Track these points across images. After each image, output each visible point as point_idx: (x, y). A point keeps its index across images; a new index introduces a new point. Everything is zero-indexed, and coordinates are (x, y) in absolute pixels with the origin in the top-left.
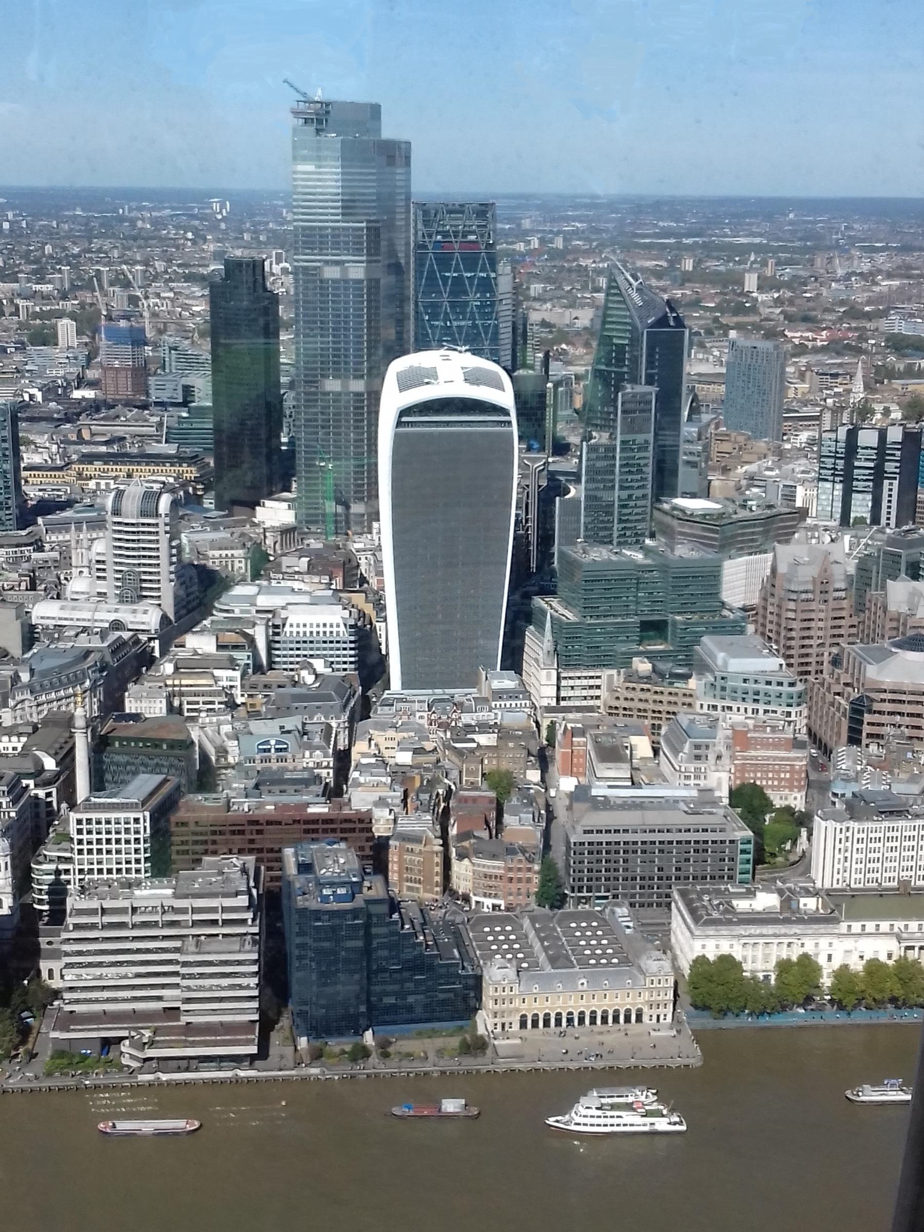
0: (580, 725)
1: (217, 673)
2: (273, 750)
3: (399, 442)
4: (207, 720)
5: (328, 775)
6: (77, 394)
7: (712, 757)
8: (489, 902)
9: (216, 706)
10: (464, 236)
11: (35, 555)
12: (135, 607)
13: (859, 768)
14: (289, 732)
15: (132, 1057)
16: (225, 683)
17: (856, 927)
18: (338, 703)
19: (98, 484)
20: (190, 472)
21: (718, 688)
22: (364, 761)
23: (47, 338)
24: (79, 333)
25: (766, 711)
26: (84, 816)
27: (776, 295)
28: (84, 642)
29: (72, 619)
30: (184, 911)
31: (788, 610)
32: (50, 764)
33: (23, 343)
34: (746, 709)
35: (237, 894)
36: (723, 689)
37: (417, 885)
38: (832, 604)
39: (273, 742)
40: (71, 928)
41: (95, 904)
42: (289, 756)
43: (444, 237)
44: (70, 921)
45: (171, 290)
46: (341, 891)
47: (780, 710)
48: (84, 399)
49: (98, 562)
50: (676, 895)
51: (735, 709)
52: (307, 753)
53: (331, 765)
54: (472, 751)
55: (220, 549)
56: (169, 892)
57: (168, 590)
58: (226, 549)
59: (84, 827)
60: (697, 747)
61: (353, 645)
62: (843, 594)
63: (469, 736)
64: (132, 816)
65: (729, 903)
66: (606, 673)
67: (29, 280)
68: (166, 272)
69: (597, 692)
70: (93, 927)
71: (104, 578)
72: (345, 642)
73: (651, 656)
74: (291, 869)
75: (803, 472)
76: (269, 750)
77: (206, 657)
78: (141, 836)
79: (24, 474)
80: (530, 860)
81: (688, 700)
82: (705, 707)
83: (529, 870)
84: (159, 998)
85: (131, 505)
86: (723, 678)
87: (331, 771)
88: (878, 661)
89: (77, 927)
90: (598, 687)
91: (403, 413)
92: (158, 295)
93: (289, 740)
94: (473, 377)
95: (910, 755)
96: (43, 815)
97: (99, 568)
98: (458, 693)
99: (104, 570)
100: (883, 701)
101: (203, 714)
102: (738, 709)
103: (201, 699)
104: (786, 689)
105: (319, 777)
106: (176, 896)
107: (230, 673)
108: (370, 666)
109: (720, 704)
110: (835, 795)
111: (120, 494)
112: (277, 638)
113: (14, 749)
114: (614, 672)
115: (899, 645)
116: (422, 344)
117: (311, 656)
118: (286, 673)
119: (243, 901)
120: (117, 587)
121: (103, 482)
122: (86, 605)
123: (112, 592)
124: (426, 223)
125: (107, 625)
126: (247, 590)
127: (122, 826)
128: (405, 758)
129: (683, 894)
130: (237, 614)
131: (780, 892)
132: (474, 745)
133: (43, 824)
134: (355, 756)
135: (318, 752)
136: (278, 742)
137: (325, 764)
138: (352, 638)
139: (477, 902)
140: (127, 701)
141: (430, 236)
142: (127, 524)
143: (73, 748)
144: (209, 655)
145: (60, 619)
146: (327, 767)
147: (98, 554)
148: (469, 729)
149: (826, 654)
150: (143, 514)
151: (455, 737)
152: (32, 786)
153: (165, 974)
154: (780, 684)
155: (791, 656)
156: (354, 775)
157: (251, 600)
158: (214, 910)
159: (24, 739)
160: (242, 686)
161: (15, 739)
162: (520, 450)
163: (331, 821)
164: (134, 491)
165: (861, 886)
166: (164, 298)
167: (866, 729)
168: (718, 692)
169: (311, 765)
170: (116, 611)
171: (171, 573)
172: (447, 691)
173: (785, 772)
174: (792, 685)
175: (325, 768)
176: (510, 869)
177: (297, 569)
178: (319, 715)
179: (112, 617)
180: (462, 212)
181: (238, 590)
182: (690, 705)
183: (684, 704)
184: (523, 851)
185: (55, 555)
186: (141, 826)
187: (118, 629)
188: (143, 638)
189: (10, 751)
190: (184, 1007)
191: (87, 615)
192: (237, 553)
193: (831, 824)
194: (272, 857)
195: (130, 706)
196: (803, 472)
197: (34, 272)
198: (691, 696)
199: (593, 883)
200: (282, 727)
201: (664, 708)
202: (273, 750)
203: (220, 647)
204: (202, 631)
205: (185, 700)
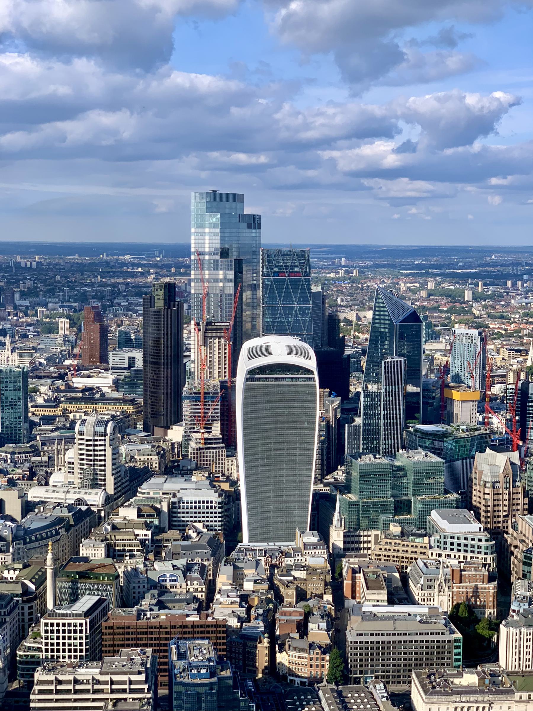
0: (357, 566)
2: (168, 581)
3: (247, 390)
5: (202, 596)
6: (67, 362)
7: (437, 587)
10: (292, 269)
11: (34, 459)
12: (91, 490)
14: (178, 569)
16: (141, 537)
17: (525, 696)
19: (75, 416)
20: (130, 409)
21: (442, 543)
22: (224, 588)
23: (52, 329)
24: (71, 326)
25: (471, 558)
26: (49, 621)
28: (58, 513)
29: (52, 498)
30: (106, 683)
31: (484, 494)
32: (33, 587)
33: (38, 332)
34: (459, 556)
35: (139, 673)
36: (445, 543)
39: (168, 576)
40: (37, 692)
41: (51, 677)
42: (178, 584)
43: (279, 269)
44: (36, 688)
45: (127, 301)
46: (203, 671)
47: (480, 556)
49: (69, 463)
50: (414, 675)
51: (453, 556)
52: (189, 582)
53: (204, 590)
55: (144, 455)
56: (98, 670)
58: (148, 455)
59: (49, 628)
60: (429, 580)
61: (220, 515)
64: (78, 622)
66: (374, 533)
67: (44, 296)
68: (125, 291)
69: (370, 545)
70: (50, 692)
71: (73, 473)
72: (215, 513)
73: (401, 523)
76: (166, 581)
77: (130, 521)
78: (83, 635)
79: (33, 410)
80: (324, 653)
81: (423, 550)
82: (434, 555)
87: (203, 594)
89: (41, 692)
90: (369, 542)
91: (252, 372)
92: (119, 304)
93: (179, 573)
94: (291, 350)
96: (26, 620)
98: (284, 545)
99: (73, 468)
102: (455, 556)
105: (195, 597)
106: (101, 673)
107: (145, 532)
108: (232, 529)
109: (444, 553)
110: (514, 611)
112: (174, 510)
113: (11, 578)
114: (379, 532)
116: (268, 331)
117: (195, 521)
119: (142, 677)
121: (78, 415)
122: (62, 489)
123: (77, 481)
124: (269, 262)
125: (73, 502)
127: (72, 628)
129: (418, 675)
130: (151, 495)
131: (478, 674)
132: (292, 578)
133: (26, 626)
134: (219, 586)
135: (195, 582)
136: (171, 575)
137: (200, 589)
139: (291, 680)
140: (81, 549)
141: (271, 269)
142: (87, 440)
143: (45, 579)
144: (133, 520)
145: (45, 498)
146: (202, 591)
147: (69, 458)
151: (280, 573)
152: (20, 602)
156: (217, 596)
158: (123, 683)
161: (12, 572)
162: (322, 395)
166: (122, 306)
170: (79, 493)
172: (277, 544)
174: (486, 541)
175: (200, 592)
176: (312, 659)
177: (189, 467)
179: (77, 496)
180: (290, 255)
181: (153, 480)
183: (421, 553)
184: (320, 647)
185: (45, 458)
186: (84, 628)
187: (79, 504)
188: (95, 510)
191: (62, 496)
192: (154, 458)
193: (513, 630)
194: (161, 649)
195: (83, 552)
197: (48, 291)
198: (425, 547)
199: (363, 668)
200: (174, 566)
201: (409, 555)
202: (168, 581)
203: (139, 516)
204: (130, 505)
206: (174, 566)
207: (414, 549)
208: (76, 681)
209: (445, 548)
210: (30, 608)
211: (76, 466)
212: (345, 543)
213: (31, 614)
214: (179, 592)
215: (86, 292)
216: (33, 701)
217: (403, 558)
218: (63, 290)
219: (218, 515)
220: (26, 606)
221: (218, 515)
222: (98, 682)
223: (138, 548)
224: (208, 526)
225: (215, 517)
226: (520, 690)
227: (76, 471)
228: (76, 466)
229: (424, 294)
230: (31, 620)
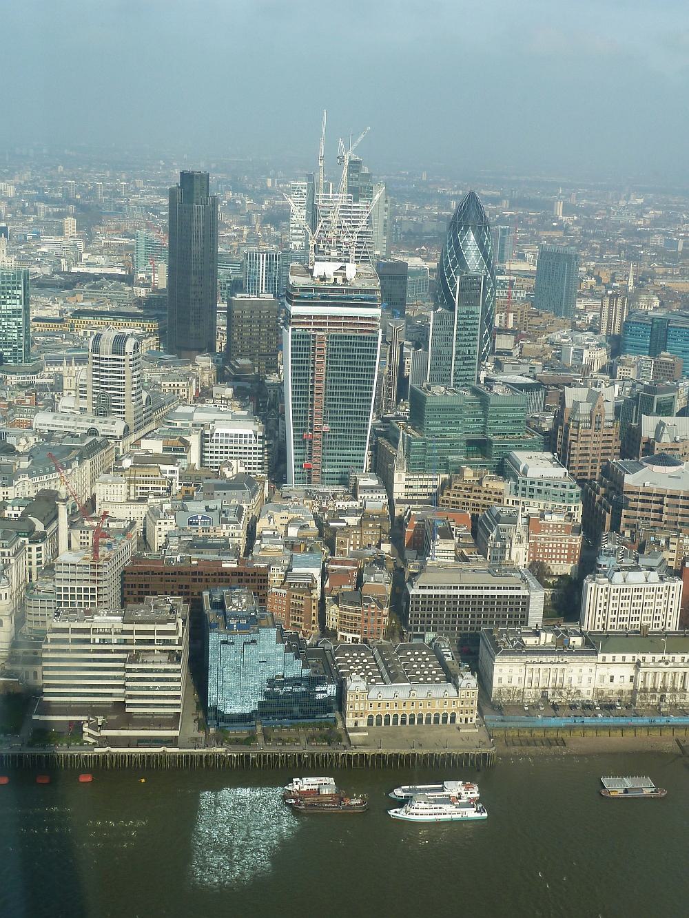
1: (162, 467)
4: (154, 501)
8: (350, 636)
9: (161, 491)
13: (617, 547)
14: (212, 510)
15: (90, 735)
16: (168, 475)
17: (609, 657)
18: (247, 492)
19: (85, 333)
22: (265, 533)
24: (78, 228)
27: (576, 218)
29: (61, 426)
30: (130, 632)
32: (40, 527)
33: (38, 233)
37: (299, 623)
38: (604, 431)
39: (200, 517)
42: (212, 527)
46: (243, 622)
47: (563, 505)
48: (79, 273)
51: (532, 504)
54: (342, 528)
57: (130, 408)
58: (174, 381)
62: (611, 424)
63: (341, 518)
65: (520, 640)
72: (255, 448)
73: (471, 465)
74: (207, 606)
75: (588, 340)
76: (197, 524)
81: (498, 497)
82: (510, 502)
83: (379, 614)
84: (110, 695)
85: (106, 346)
86: (523, 482)
88: (634, 471)
89: (54, 641)
93: (213, 516)
95: (652, 539)
97: (81, 391)
99: (86, 391)
100: (636, 500)
101: (150, 496)
103: (150, 486)
104: (568, 490)
106: (124, 622)
107: (171, 468)
109: (522, 500)
111: (98, 337)
112: (206, 444)
114: (447, 476)
115: (647, 462)
118: (212, 470)
120: (94, 404)
123: (90, 408)
126: (189, 410)
128: (293, 532)
130: (179, 426)
131: (557, 633)
132: (344, 524)
135: (232, 525)
136: (203, 518)
138: (261, 446)
144: (158, 454)
145: (53, 426)
147: (82, 380)
148: (342, 512)
149: (598, 467)
150: (114, 353)
152: (27, 542)
153: (115, 678)
154: (564, 486)
155: (573, 468)
157: (189, 416)
158: (152, 633)
159: (22, 509)
160: (180, 477)
163: (240, 574)
164: (109, 335)
165: (614, 630)
167: (623, 520)
168: (520, 491)
169: (227, 535)
170: (93, 421)
171: (133, 395)
173: (565, 549)
174: (571, 487)
177: (223, 396)
178: (234, 500)
179: (90, 425)
182: (499, 501)
183: (495, 500)
185: (51, 381)
187: (93, 435)
189: (13, 516)
190: (128, 701)
192: (181, 384)
196: (588, 340)
198: (500, 494)
200: (207, 508)
201: (482, 501)
203: (165, 450)
205: (139, 485)
206: (207, 508)
207: (487, 496)
208: (96, 631)
209: (523, 495)
210: (39, 549)
211: (89, 389)
212: (406, 486)
213: (39, 556)
214: (212, 536)
215: (95, 187)
216: (46, 651)
217: (474, 505)
218: (66, 184)
219: (257, 451)
220: (34, 547)
221: (257, 451)
222: (124, 632)
223: (164, 486)
224: (246, 463)
225: (255, 453)
226: (603, 652)
227: (89, 395)
228: (89, 389)
229: (505, 203)
230: (39, 563)
